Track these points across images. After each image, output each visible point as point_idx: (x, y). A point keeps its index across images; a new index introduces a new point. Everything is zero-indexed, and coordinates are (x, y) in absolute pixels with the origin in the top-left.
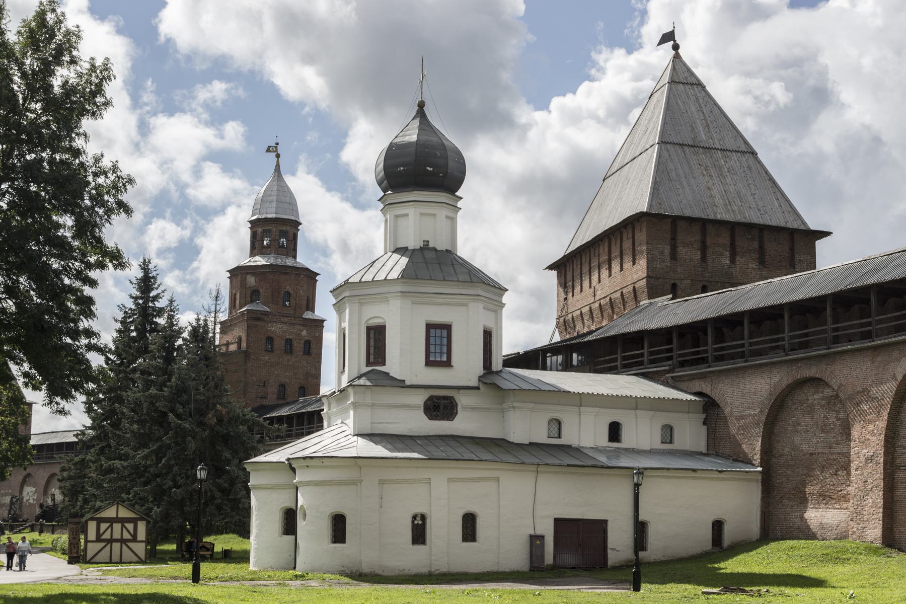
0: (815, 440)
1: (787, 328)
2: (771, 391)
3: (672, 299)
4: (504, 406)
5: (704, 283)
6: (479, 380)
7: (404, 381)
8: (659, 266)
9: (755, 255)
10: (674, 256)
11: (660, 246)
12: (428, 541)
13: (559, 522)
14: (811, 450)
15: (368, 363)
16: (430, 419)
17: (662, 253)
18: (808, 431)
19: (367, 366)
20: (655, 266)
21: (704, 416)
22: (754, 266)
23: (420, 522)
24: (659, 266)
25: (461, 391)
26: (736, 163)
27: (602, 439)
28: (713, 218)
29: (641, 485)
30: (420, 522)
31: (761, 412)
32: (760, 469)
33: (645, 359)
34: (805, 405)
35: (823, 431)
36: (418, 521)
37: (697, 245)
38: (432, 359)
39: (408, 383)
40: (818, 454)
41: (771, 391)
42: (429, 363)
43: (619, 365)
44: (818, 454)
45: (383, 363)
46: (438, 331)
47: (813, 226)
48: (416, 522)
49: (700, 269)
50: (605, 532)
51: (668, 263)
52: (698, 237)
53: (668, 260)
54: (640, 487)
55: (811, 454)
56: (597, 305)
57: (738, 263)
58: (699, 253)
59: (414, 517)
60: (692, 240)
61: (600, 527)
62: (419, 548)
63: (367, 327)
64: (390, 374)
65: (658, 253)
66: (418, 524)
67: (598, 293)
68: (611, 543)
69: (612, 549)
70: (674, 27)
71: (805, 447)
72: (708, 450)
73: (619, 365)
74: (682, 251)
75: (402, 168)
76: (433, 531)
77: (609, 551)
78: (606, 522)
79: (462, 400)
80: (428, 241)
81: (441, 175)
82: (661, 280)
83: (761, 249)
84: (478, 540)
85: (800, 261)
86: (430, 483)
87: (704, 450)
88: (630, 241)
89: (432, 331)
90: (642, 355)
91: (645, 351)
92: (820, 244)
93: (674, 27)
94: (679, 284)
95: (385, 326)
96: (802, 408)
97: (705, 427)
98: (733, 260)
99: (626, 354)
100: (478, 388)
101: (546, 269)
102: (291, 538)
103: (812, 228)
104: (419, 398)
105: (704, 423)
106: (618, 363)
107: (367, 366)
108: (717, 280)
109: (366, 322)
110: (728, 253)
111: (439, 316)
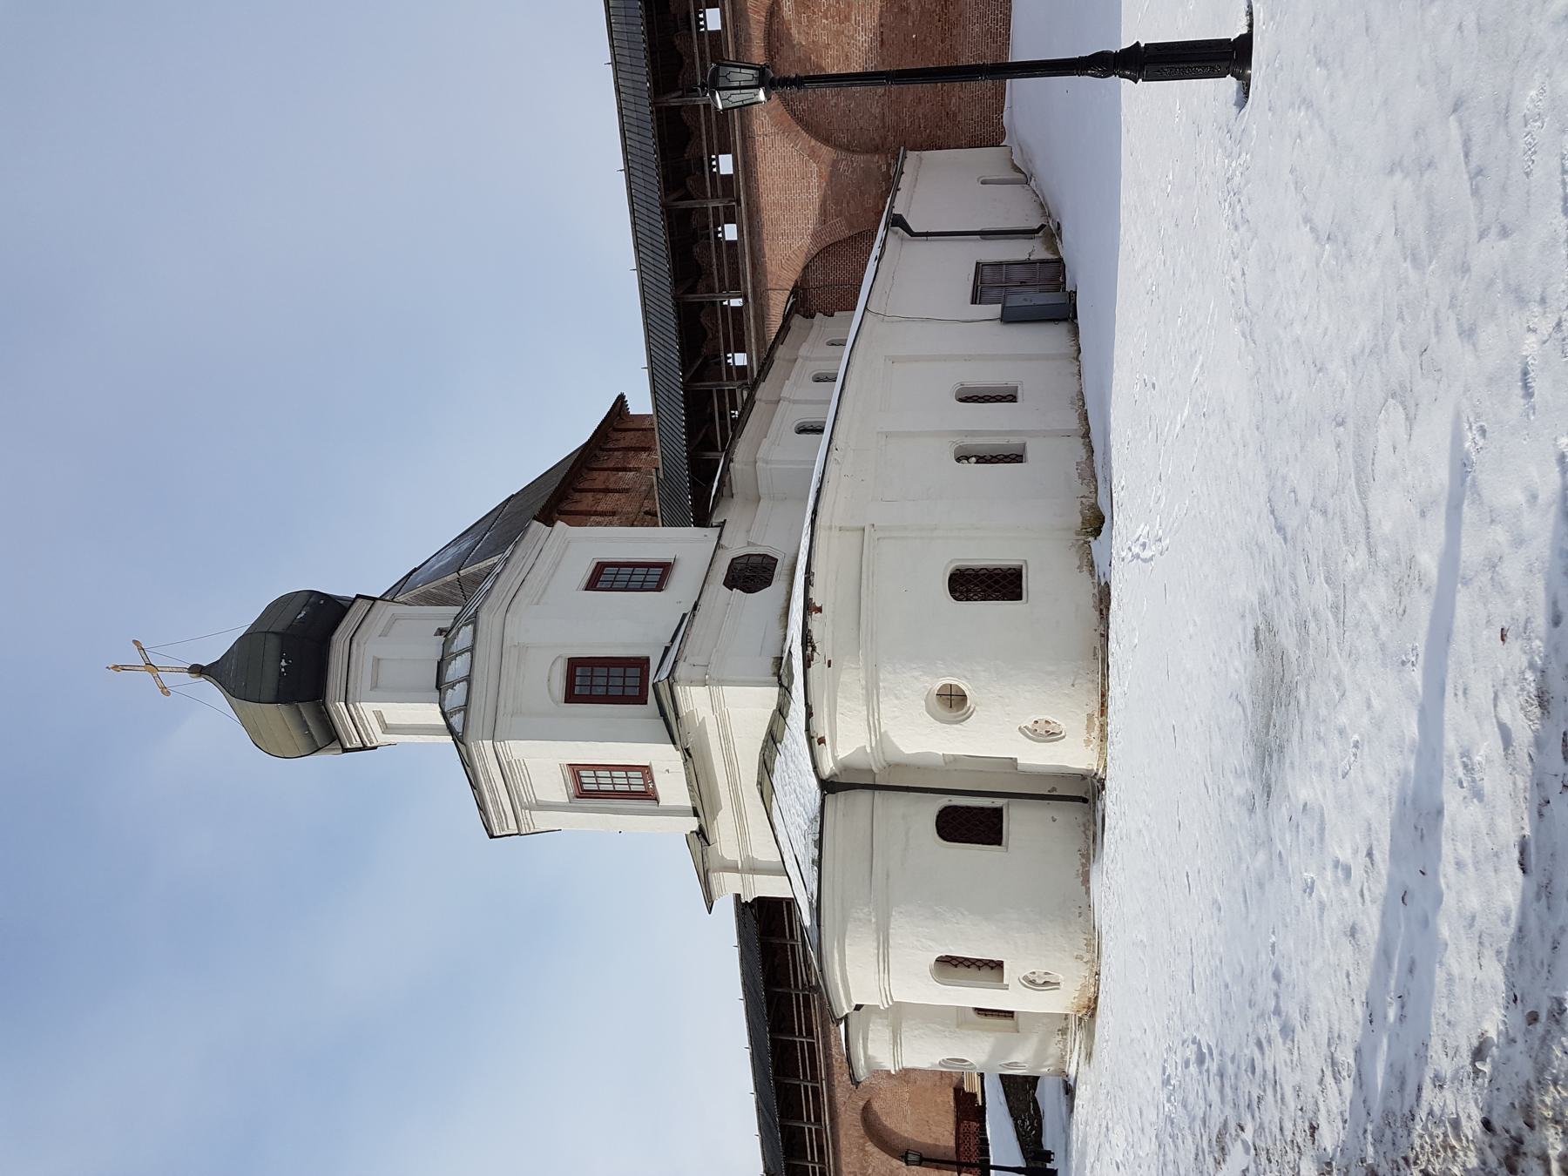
12: (1015, 440)
15: (642, 700)
21: (819, 315)
35: (847, 18)
37: (600, 496)
43: (817, 1127)
45: (643, 663)
62: (1029, 454)
63: (565, 702)
73: (817, 1127)
74: (601, 507)
75: (283, 663)
81: (322, 602)
84: (1012, 384)
102: (1016, 820)
105: (832, 316)
109: (557, 703)
110: (620, 473)
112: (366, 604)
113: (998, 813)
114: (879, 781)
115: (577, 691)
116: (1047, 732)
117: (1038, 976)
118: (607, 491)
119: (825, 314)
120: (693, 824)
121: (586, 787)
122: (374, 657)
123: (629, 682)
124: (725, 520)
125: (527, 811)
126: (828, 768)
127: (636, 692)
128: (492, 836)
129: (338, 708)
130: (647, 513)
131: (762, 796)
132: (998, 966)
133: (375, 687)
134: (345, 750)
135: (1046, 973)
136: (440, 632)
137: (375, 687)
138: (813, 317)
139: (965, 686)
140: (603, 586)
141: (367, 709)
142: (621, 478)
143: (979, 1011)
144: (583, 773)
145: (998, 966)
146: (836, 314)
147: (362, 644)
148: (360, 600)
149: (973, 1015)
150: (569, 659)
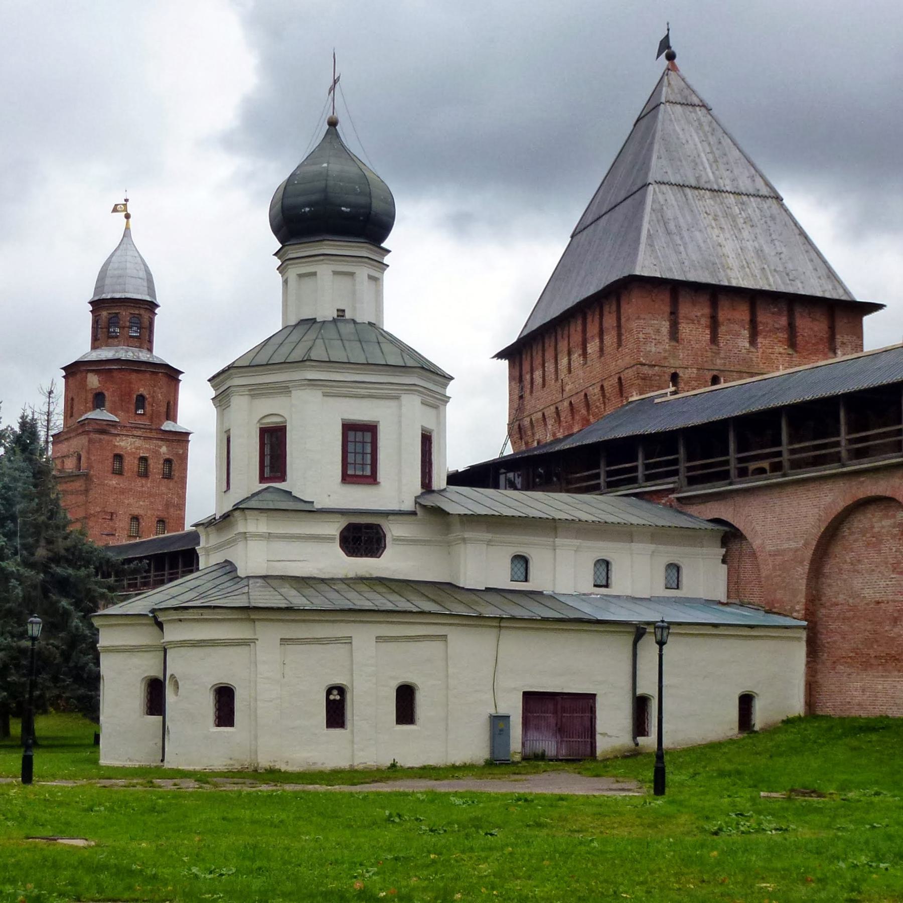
0: (882, 583)
2: (820, 515)
4: (452, 536)
5: (715, 373)
6: (416, 502)
7: (313, 502)
8: (653, 349)
9: (783, 335)
10: (674, 334)
11: (655, 322)
12: (348, 723)
13: (529, 697)
14: (878, 597)
15: (262, 479)
17: (658, 331)
18: (873, 570)
19: (260, 482)
20: (648, 349)
21: (723, 551)
22: (781, 350)
23: (338, 697)
24: (653, 349)
25: (390, 517)
26: (755, 211)
27: (586, 585)
28: (726, 284)
29: (665, 643)
30: (338, 697)
31: (806, 545)
32: (805, 623)
33: (640, 473)
34: (868, 535)
36: (335, 696)
37: (705, 321)
38: (350, 472)
39: (317, 506)
40: (888, 603)
41: (820, 515)
42: (346, 478)
44: (888, 603)
45: (282, 478)
46: (359, 434)
47: (859, 298)
48: (332, 697)
49: (709, 354)
50: (592, 710)
51: (667, 345)
53: (667, 341)
54: (664, 647)
55: (878, 603)
56: (566, 404)
57: (760, 345)
58: (708, 331)
59: (329, 691)
60: (699, 314)
61: (587, 701)
64: (293, 494)
65: (652, 332)
66: (334, 700)
67: (567, 388)
68: (600, 727)
69: (601, 734)
70: (668, 30)
71: (869, 594)
72: (728, 597)
74: (685, 329)
75: (307, 209)
76: (354, 710)
77: (598, 738)
78: (593, 696)
79: (393, 530)
80: (343, 311)
81: (361, 218)
82: (656, 368)
83: (791, 328)
85: (843, 343)
86: (351, 643)
87: (724, 599)
88: (614, 316)
89: (351, 435)
90: (635, 469)
91: (640, 463)
92: (869, 321)
93: (668, 30)
94: (681, 374)
95: (285, 427)
96: (864, 538)
97: (725, 566)
98: (753, 341)
99: (612, 468)
100: (414, 513)
103: (858, 300)
104: (334, 528)
106: (602, 481)
107: (260, 482)
108: (732, 369)
111: (361, 412)
118: (714, 325)
119: (724, 556)
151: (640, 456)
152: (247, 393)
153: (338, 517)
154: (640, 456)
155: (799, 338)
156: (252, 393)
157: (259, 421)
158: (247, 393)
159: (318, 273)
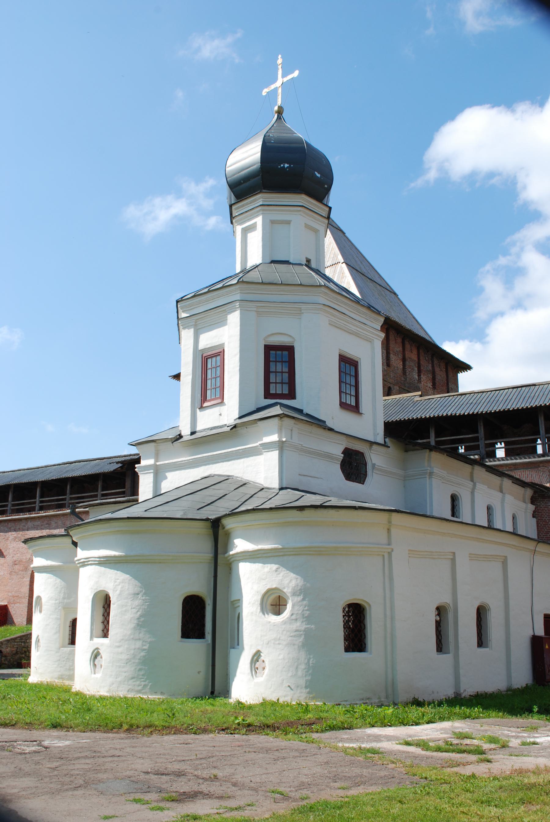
1: (68, 492)
3: (421, 396)
9: (430, 376)
12: (452, 647)
15: (267, 395)
16: (346, 479)
19: (265, 398)
37: (401, 356)
45: (292, 395)
49: (403, 379)
52: (401, 349)
63: (265, 345)
75: (286, 165)
81: (326, 186)
101: (170, 376)
105: (533, 517)
107: (265, 398)
112: (325, 214)
113: (201, 636)
114: (220, 557)
115: (272, 352)
116: (257, 668)
117: (99, 661)
118: (404, 360)
119: (534, 512)
120: (186, 431)
121: (209, 361)
122: (291, 221)
123: (279, 386)
124: (389, 447)
125: (194, 323)
126: (229, 523)
127: (272, 391)
128: (177, 302)
129: (259, 199)
130: (390, 389)
131: (205, 478)
132: (105, 634)
133: (273, 222)
134: (231, 206)
135: (101, 666)
136: (308, 261)
137: (273, 222)
138: (532, 503)
139: (286, 614)
140: (342, 366)
141: (259, 220)
142: (413, 369)
143: (74, 623)
144: (218, 358)
145: (105, 634)
146: (535, 519)
147: (300, 213)
148: (327, 209)
149: (73, 617)
150: (293, 346)
151: (432, 434)
152: (255, 309)
153: (343, 438)
154: (432, 434)
155: (437, 379)
156: (260, 310)
157: (266, 337)
158: (255, 309)
159: (292, 223)
